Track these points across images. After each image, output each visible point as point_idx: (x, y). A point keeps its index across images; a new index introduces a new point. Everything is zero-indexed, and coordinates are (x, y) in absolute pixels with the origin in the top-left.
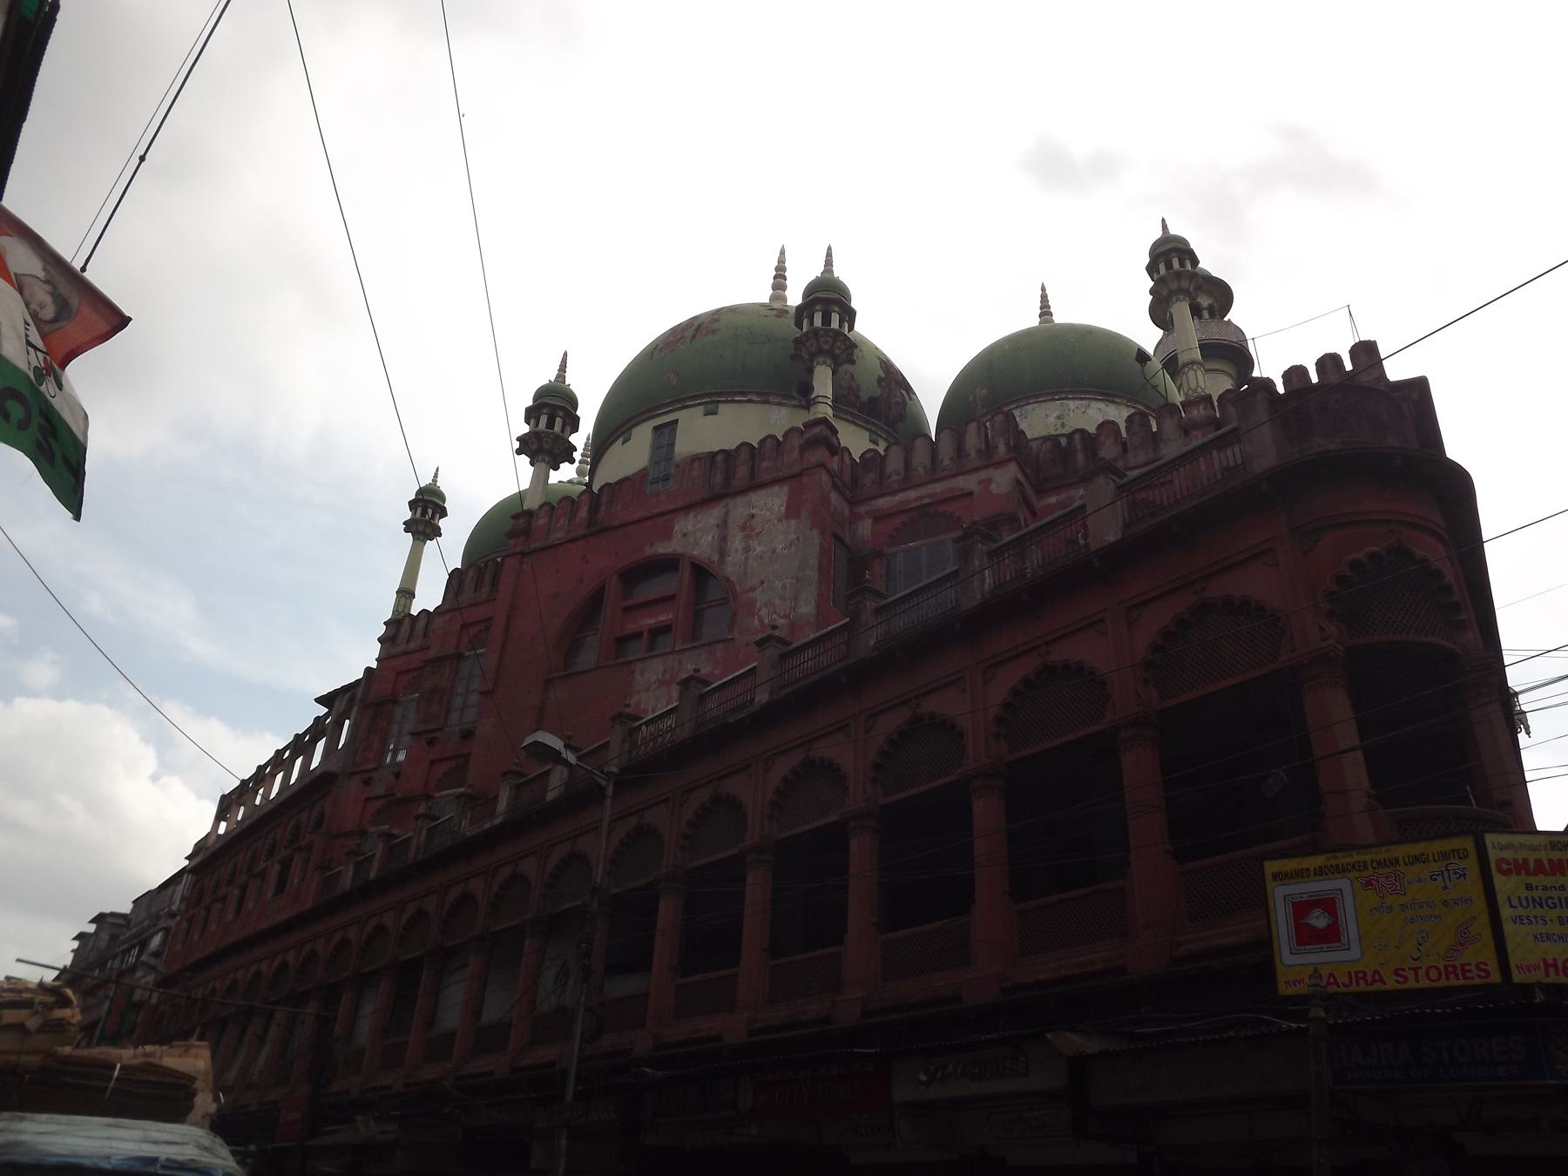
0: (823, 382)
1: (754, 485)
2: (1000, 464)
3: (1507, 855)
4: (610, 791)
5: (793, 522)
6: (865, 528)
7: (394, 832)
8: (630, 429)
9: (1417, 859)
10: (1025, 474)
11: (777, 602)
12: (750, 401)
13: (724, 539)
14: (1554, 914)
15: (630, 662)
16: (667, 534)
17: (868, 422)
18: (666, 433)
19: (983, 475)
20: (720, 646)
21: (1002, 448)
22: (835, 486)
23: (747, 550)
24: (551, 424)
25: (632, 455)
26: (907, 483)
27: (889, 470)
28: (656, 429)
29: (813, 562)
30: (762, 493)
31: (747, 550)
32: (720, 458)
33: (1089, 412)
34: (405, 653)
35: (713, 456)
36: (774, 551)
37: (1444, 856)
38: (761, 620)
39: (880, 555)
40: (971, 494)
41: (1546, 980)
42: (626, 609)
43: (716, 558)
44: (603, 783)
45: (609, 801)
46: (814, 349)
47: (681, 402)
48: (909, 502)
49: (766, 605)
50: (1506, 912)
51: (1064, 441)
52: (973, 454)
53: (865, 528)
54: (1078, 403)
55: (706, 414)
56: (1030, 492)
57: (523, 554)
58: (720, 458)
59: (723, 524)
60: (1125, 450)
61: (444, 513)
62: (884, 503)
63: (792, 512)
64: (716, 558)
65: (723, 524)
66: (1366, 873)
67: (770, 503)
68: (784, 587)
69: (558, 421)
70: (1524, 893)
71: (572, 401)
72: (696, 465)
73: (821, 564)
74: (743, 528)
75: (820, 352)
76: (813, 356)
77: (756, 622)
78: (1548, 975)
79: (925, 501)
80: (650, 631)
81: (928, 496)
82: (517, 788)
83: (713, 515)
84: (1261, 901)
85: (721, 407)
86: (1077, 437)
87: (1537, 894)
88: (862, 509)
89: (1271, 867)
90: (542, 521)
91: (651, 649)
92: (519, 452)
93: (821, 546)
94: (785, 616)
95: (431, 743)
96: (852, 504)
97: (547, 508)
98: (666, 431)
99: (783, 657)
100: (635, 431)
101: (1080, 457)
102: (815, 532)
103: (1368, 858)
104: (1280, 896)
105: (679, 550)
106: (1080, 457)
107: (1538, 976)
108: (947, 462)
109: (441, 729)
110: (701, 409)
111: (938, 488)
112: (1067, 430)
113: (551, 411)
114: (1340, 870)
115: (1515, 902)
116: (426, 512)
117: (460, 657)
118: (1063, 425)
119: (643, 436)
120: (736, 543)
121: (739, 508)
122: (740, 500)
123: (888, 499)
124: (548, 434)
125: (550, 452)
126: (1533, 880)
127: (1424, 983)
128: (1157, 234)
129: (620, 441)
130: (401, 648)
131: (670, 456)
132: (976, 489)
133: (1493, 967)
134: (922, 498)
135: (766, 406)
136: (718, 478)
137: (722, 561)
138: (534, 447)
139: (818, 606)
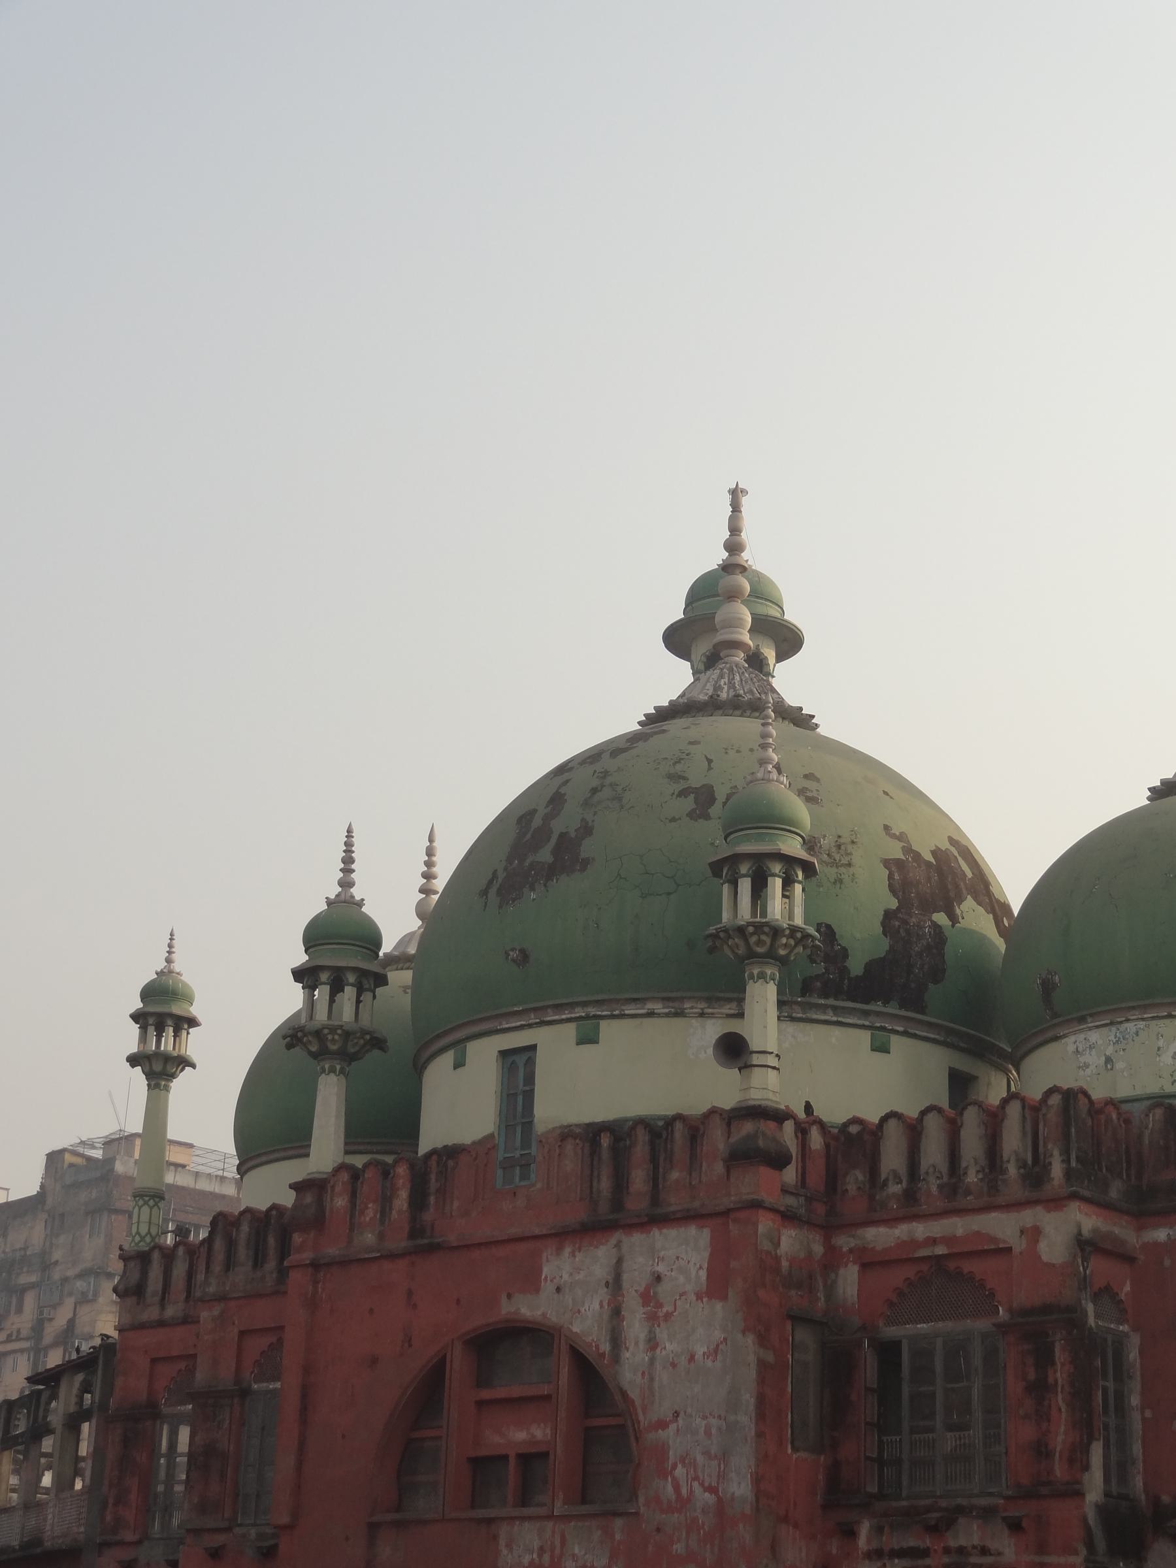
1: (657, 1218)
2: (1055, 1203)
5: (719, 1306)
11: (700, 1459)
12: (651, 1014)
13: (616, 1312)
15: (490, 1521)
16: (531, 1281)
17: (866, 1014)
18: (519, 1067)
19: (1028, 1217)
20: (619, 1523)
21: (1057, 1170)
23: (652, 1344)
26: (911, 1205)
28: (504, 1054)
29: (748, 1399)
30: (672, 1233)
31: (652, 1344)
32: (605, 1141)
34: (161, 1324)
35: (593, 1133)
36: (692, 1358)
38: (677, 1488)
40: (1009, 1250)
42: (480, 1404)
47: (540, 1012)
48: (914, 1244)
49: (683, 1460)
52: (1012, 1170)
58: (605, 1141)
59: (615, 1284)
62: (880, 1237)
63: (716, 1287)
64: (606, 1347)
65: (615, 1284)
67: (679, 1256)
68: (708, 1433)
72: (569, 1146)
73: (761, 1400)
74: (647, 1297)
77: (670, 1488)
79: (940, 1250)
80: (520, 1456)
83: (595, 1261)
85: (603, 1024)
88: (844, 1242)
93: (762, 1365)
94: (712, 1490)
96: (829, 1227)
97: (345, 1176)
98: (521, 1060)
102: (750, 1339)
105: (554, 1318)
110: (570, 1030)
111: (958, 1226)
116: (163, 1012)
117: (245, 1393)
120: (635, 1327)
123: (882, 1230)
130: (151, 1313)
131: (528, 1125)
137: (616, 1359)
139: (757, 1480)
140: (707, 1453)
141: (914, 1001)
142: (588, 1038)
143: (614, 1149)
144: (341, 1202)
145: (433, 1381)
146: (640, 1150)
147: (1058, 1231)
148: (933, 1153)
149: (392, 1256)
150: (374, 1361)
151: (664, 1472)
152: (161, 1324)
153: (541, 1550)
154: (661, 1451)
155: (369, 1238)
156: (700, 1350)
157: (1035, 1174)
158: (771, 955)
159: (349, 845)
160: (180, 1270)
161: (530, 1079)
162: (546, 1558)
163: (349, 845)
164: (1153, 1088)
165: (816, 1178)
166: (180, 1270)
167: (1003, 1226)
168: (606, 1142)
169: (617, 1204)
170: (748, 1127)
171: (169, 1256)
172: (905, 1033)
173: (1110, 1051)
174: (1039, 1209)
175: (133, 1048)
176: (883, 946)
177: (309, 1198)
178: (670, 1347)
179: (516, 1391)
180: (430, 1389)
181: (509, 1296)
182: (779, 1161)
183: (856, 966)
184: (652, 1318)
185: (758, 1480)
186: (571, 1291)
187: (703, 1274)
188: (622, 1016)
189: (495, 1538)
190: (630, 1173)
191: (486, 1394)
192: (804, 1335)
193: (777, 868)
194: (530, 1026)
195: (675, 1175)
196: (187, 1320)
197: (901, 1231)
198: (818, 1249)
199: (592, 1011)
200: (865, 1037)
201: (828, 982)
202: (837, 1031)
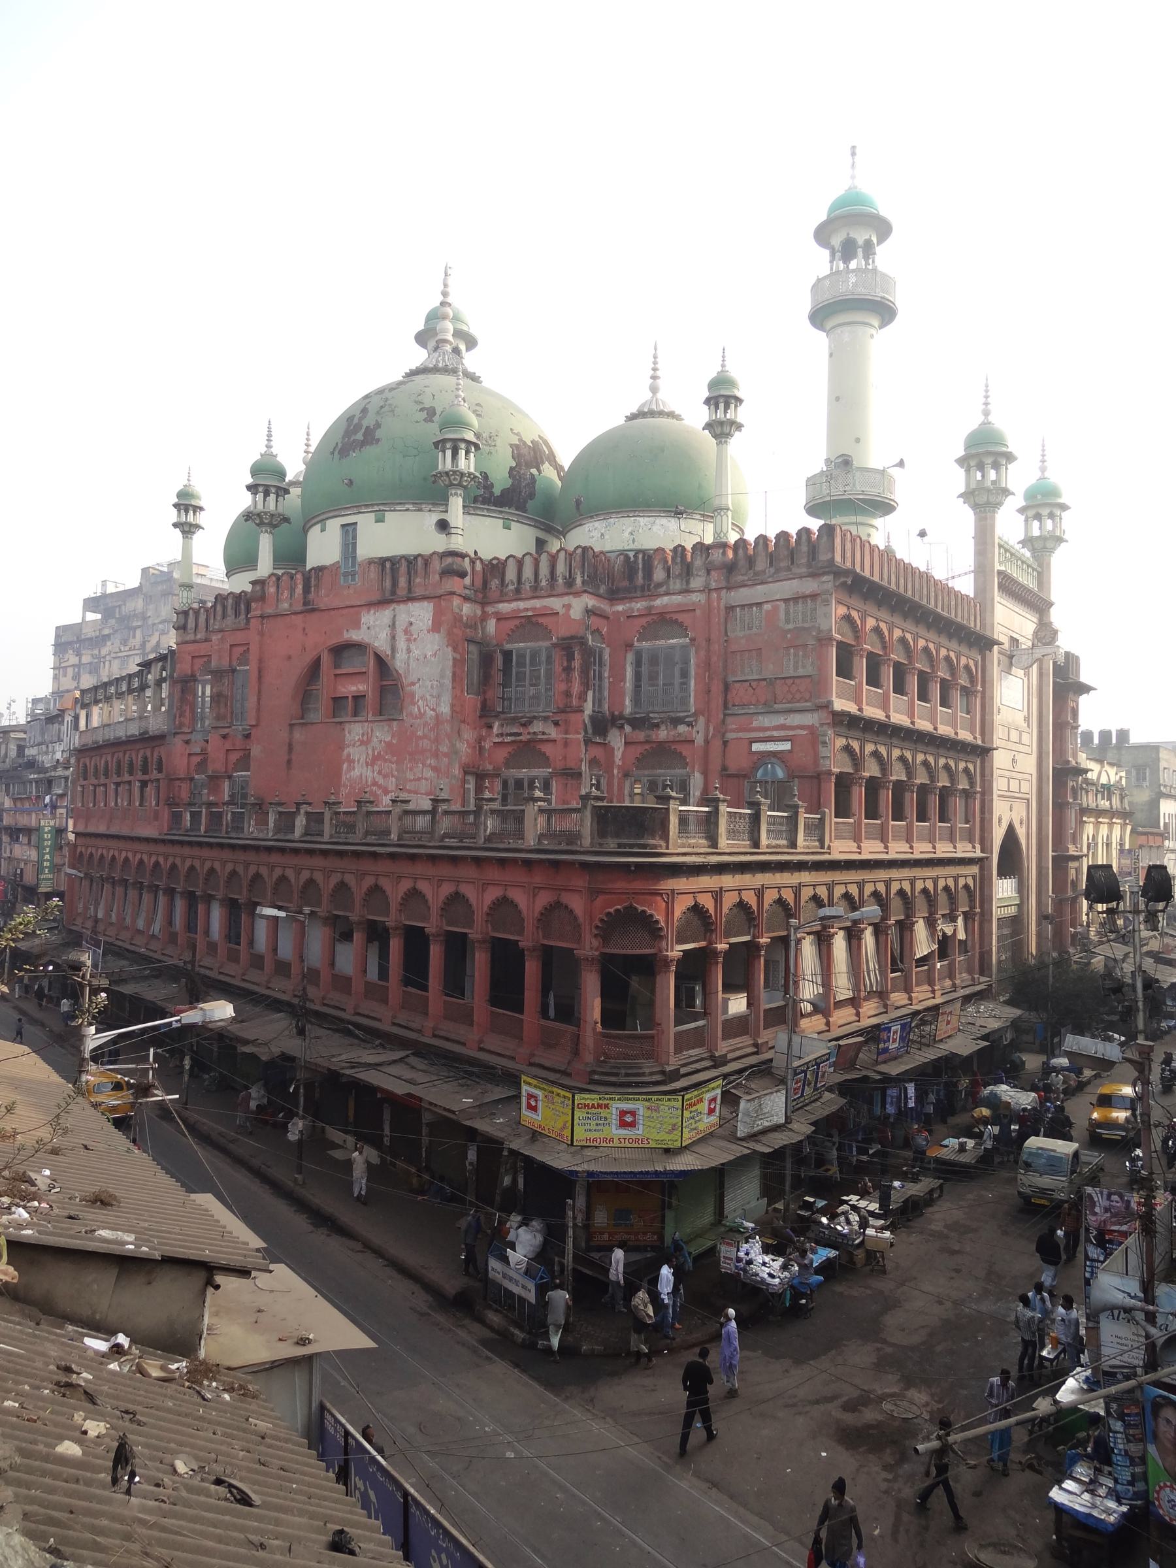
1: (410, 599)
2: (577, 594)
5: (437, 635)
6: (491, 626)
9: (558, 1095)
10: (599, 596)
12: (407, 510)
13: (393, 638)
15: (341, 723)
16: (357, 625)
17: (501, 512)
18: (349, 531)
19: (566, 600)
20: (395, 723)
21: (579, 580)
23: (409, 651)
26: (518, 594)
28: (343, 526)
29: (449, 673)
30: (417, 604)
31: (409, 651)
32: (388, 565)
33: (655, 528)
34: (195, 642)
35: (383, 561)
38: (419, 709)
42: (336, 675)
47: (359, 507)
48: (519, 610)
51: (631, 554)
52: (560, 580)
53: (491, 626)
54: (646, 519)
58: (388, 565)
59: (393, 626)
60: (669, 576)
62: (505, 607)
63: (436, 627)
64: (389, 652)
65: (393, 626)
67: (420, 614)
73: (454, 674)
74: (406, 632)
79: (530, 613)
81: (534, 609)
88: (490, 609)
93: (454, 659)
94: (433, 710)
96: (483, 604)
97: (274, 579)
98: (350, 529)
101: (640, 574)
102: (450, 649)
105: (367, 640)
106: (640, 574)
111: (537, 603)
116: (186, 504)
117: (234, 671)
118: (634, 541)
120: (401, 644)
123: (506, 604)
130: (191, 637)
131: (354, 558)
132: (562, 611)
137: (393, 657)
139: (453, 706)
141: (522, 507)
142: (380, 520)
143: (392, 569)
144: (272, 590)
145: (316, 664)
146: (403, 569)
147: (578, 605)
148: (528, 572)
149: (296, 613)
151: (414, 703)
152: (195, 642)
154: (413, 695)
155: (286, 605)
157: (570, 582)
158: (460, 485)
160: (202, 618)
161: (355, 537)
164: (620, 548)
165: (479, 582)
166: (202, 618)
167: (555, 604)
168: (389, 566)
169: (393, 593)
170: (449, 560)
171: (197, 612)
175: (175, 520)
176: (509, 483)
177: (258, 588)
178: (416, 652)
179: (351, 670)
180: (314, 669)
182: (463, 575)
183: (497, 491)
184: (409, 640)
186: (374, 629)
190: (398, 578)
191: (338, 672)
192: (473, 648)
193: (463, 445)
195: (418, 580)
196: (206, 640)
197: (514, 605)
198: (479, 612)
199: (382, 508)
201: (487, 498)
202: (488, 519)
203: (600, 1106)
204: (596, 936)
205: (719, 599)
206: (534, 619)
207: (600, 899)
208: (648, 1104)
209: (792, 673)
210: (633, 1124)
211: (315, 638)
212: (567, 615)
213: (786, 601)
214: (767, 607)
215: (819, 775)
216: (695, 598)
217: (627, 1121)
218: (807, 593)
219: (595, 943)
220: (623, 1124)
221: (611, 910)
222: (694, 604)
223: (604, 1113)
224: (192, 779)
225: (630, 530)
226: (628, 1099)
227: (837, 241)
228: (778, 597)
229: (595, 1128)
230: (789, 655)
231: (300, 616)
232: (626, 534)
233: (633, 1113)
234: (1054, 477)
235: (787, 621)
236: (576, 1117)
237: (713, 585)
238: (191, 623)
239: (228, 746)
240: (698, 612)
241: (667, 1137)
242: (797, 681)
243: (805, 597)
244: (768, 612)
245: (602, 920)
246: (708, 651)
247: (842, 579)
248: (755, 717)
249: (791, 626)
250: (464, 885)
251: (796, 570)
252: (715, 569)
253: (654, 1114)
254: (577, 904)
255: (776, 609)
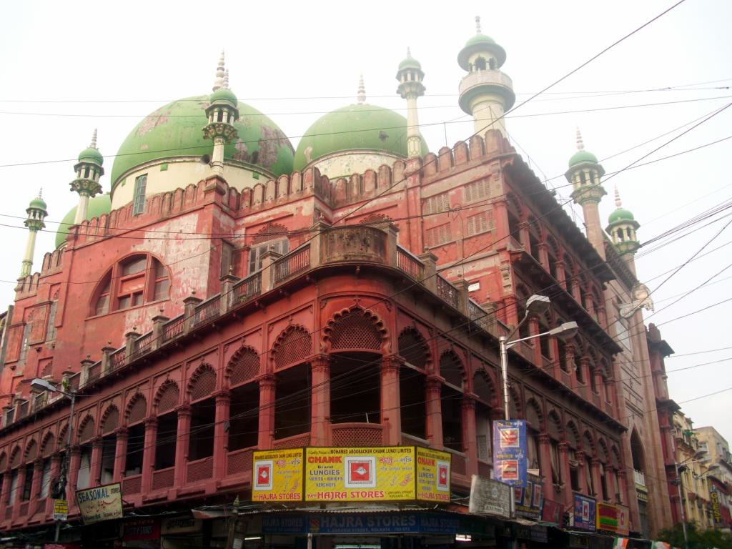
0: (218, 153)
2: (307, 198)
3: (314, 455)
4: (73, 402)
7: (24, 398)
8: (125, 178)
9: (290, 456)
10: (323, 203)
12: (184, 161)
14: (326, 477)
16: (141, 239)
17: (252, 167)
18: (141, 181)
19: (299, 204)
22: (223, 211)
24: (87, 175)
25: (125, 195)
27: (255, 200)
28: (137, 178)
32: (167, 196)
33: (364, 161)
36: (190, 251)
37: (296, 455)
39: (249, 249)
40: (292, 215)
41: (317, 500)
42: (123, 281)
43: (163, 255)
44: (70, 398)
45: (73, 406)
46: (213, 134)
47: (148, 164)
48: (263, 219)
49: (185, 282)
50: (308, 476)
51: (348, 179)
52: (295, 193)
55: (162, 170)
56: (327, 212)
57: (74, 250)
58: (167, 196)
60: (376, 187)
61: (46, 214)
62: (250, 220)
63: (198, 231)
66: (277, 459)
67: (189, 223)
68: (194, 272)
69: (91, 172)
70: (317, 469)
71: (99, 159)
72: (156, 200)
73: (211, 259)
75: (217, 135)
76: (214, 138)
77: (181, 291)
78: (319, 497)
81: (273, 216)
82: (90, 370)
84: (251, 468)
86: (354, 178)
87: (321, 470)
88: (240, 223)
89: (256, 454)
90: (82, 231)
91: (134, 303)
92: (72, 190)
93: (212, 249)
95: (39, 350)
96: (236, 219)
99: (165, 326)
100: (128, 178)
103: (278, 453)
104: (257, 464)
105: (147, 250)
107: (316, 499)
108: (282, 196)
109: (43, 343)
110: (159, 167)
111: (277, 211)
112: (351, 173)
113: (90, 165)
114: (271, 457)
115: (313, 473)
117: (51, 303)
118: (349, 170)
119: (131, 181)
121: (175, 226)
122: (175, 221)
124: (85, 181)
125: (87, 190)
126: (321, 465)
127: (285, 500)
128: (404, 57)
129: (121, 184)
131: (143, 196)
133: (301, 495)
134: (269, 216)
135: (193, 164)
136: (166, 209)
138: (79, 188)
140: (193, 278)
142: (165, 169)
148: (270, 194)
150: (90, 273)
151: (179, 286)
153: (139, 317)
154: (179, 280)
156: (193, 249)
159: (95, 135)
160: (35, 281)
162: (140, 319)
163: (95, 135)
164: (340, 175)
166: (35, 281)
167: (290, 209)
168: (169, 198)
172: (263, 175)
173: (326, 167)
174: (302, 202)
180: (106, 281)
181: (134, 246)
185: (209, 283)
186: (153, 243)
187: (195, 227)
188: (175, 162)
189: (125, 316)
191: (125, 278)
192: (226, 248)
194: (146, 168)
195: (188, 201)
197: (259, 216)
199: (166, 161)
200: (252, 173)
202: (242, 171)
203: (332, 460)
204: (325, 339)
205: (415, 194)
206: (274, 223)
207: (330, 304)
208: (381, 455)
209: (475, 234)
210: (365, 478)
211: (107, 257)
212: (300, 215)
213: (466, 185)
214: (451, 193)
215: (503, 300)
216: (397, 197)
217: (359, 474)
218: (482, 175)
219: (323, 344)
220: (356, 477)
221: (340, 312)
222: (396, 201)
223: (336, 466)
224: (13, 396)
225: (345, 164)
226: (359, 452)
227: (472, 60)
228: (460, 184)
229: (326, 482)
230: (472, 222)
231: (100, 244)
232: (344, 166)
233: (365, 466)
234: (627, 207)
235: (468, 199)
236: (307, 472)
237: (410, 185)
238: (27, 287)
239: (41, 356)
240: (400, 206)
241: (400, 489)
242: (480, 238)
243: (479, 180)
244: (453, 196)
245: (331, 323)
246: (409, 230)
247: (507, 162)
248: (449, 271)
249: (471, 202)
250: (209, 356)
251: (472, 163)
252: (410, 175)
253: (387, 466)
254: (307, 321)
255: (459, 193)
